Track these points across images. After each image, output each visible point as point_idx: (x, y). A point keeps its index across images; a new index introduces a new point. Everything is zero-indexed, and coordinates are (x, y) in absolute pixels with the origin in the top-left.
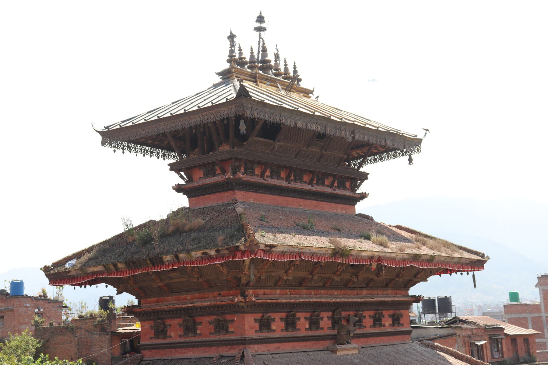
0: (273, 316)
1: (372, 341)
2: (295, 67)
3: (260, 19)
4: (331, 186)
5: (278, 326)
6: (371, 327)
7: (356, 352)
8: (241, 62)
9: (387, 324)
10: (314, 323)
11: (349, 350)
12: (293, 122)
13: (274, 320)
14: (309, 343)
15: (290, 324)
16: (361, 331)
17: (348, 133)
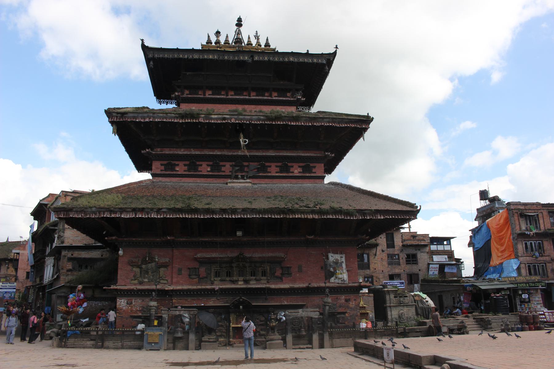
0: (177, 163)
2: (267, 40)
3: (240, 20)
4: (271, 96)
5: (181, 168)
6: (277, 172)
7: (250, 185)
8: (218, 42)
9: (296, 171)
10: (216, 167)
11: (240, 183)
12: (191, 56)
13: (178, 165)
14: (209, 179)
16: (265, 175)
17: (246, 58)
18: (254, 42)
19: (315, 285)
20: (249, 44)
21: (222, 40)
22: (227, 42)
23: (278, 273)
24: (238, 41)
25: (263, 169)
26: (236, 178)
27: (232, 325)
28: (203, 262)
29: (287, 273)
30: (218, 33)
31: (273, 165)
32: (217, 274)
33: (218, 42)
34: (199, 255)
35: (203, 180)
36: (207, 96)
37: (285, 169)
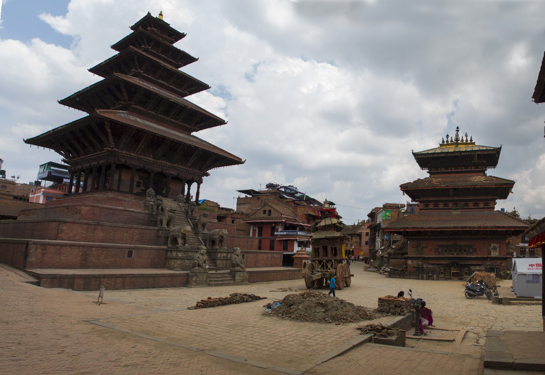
1: (471, 210)
3: (458, 128)
8: (447, 141)
10: (446, 205)
15: (436, 205)
18: (465, 139)
19: (486, 256)
20: (462, 140)
21: (449, 140)
22: (451, 141)
23: (471, 251)
24: (457, 140)
25: (467, 205)
26: (455, 210)
27: (452, 272)
28: (440, 246)
29: (475, 251)
30: (448, 136)
31: (471, 203)
32: (446, 251)
33: (447, 141)
34: (438, 244)
35: (440, 211)
36: (443, 171)
37: (476, 204)
